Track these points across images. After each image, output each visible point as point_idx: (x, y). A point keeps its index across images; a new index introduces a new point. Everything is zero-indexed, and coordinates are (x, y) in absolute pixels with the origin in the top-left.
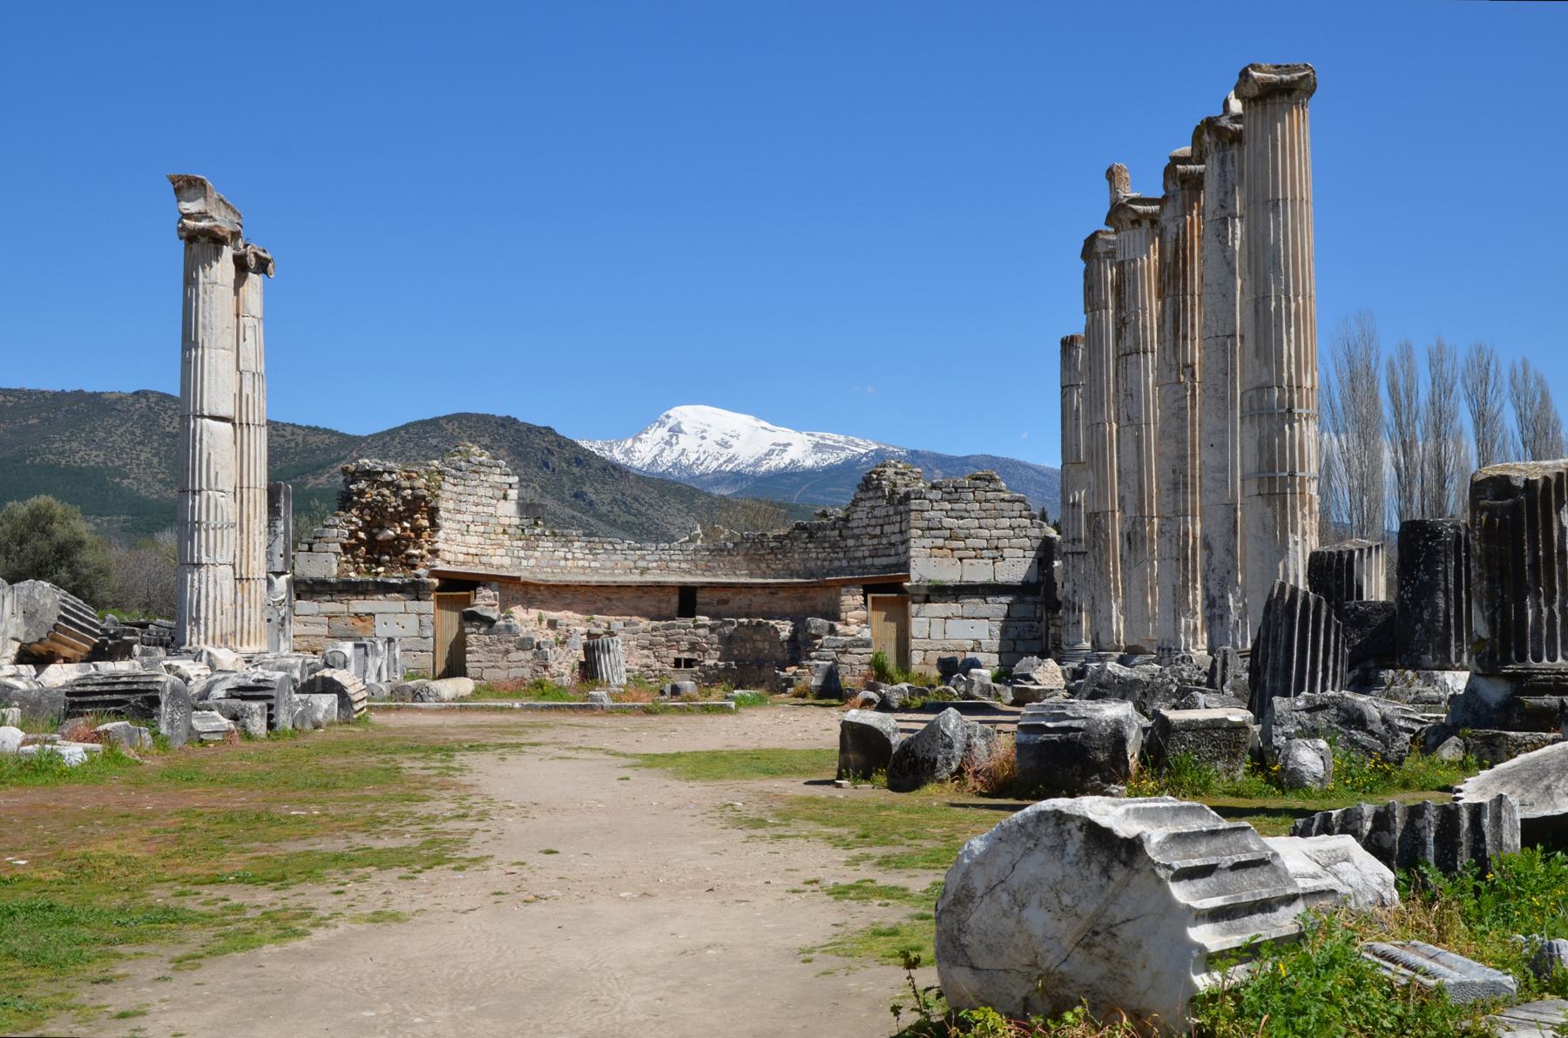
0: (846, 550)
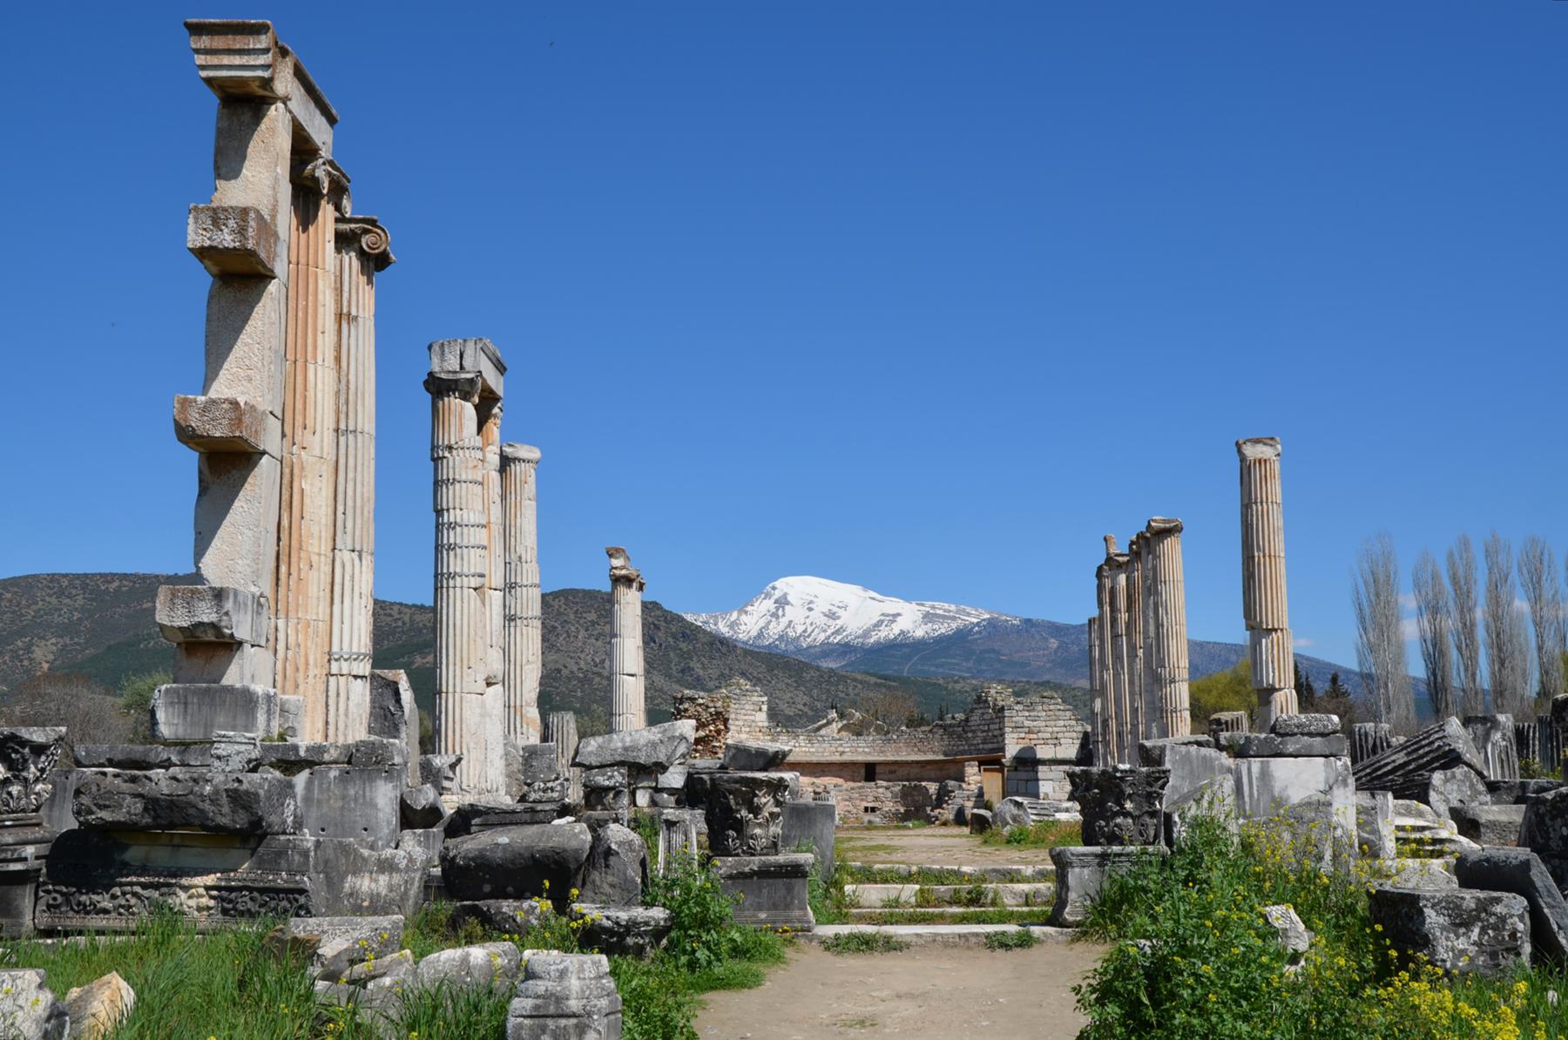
0: (967, 739)
